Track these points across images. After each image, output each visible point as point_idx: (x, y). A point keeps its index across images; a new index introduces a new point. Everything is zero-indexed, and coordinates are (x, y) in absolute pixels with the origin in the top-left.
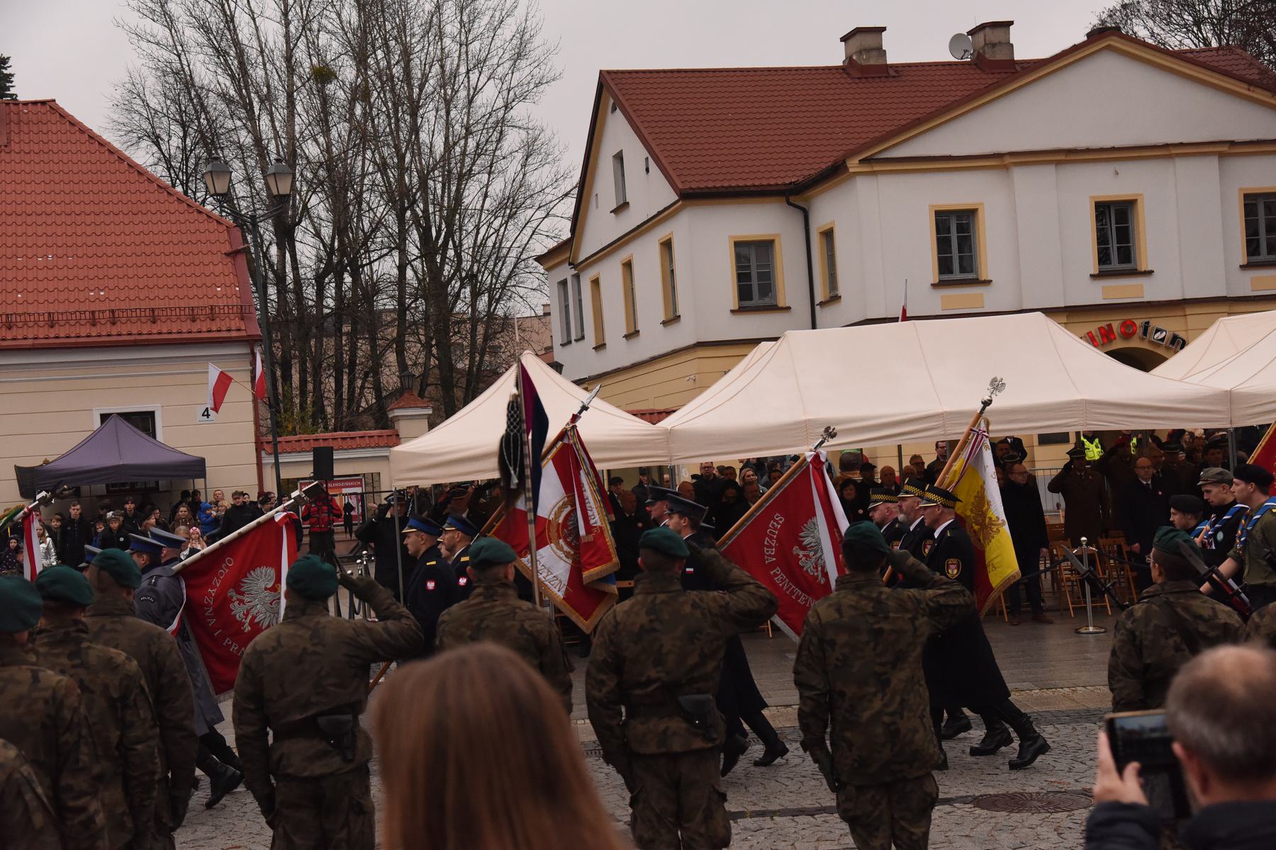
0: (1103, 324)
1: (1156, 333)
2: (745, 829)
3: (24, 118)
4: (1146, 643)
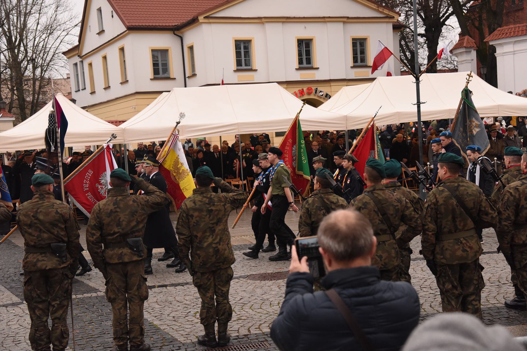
0: (300, 89)
2: (155, 292)
4: (312, 213)
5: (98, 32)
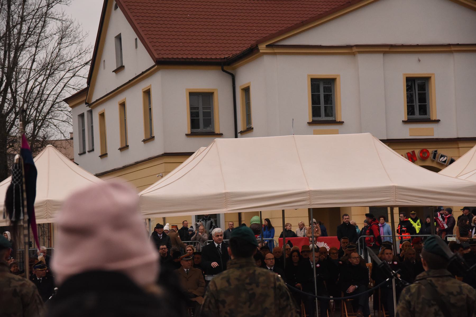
0: (410, 151)
1: (441, 158)
4: (417, 310)
5: (115, 68)
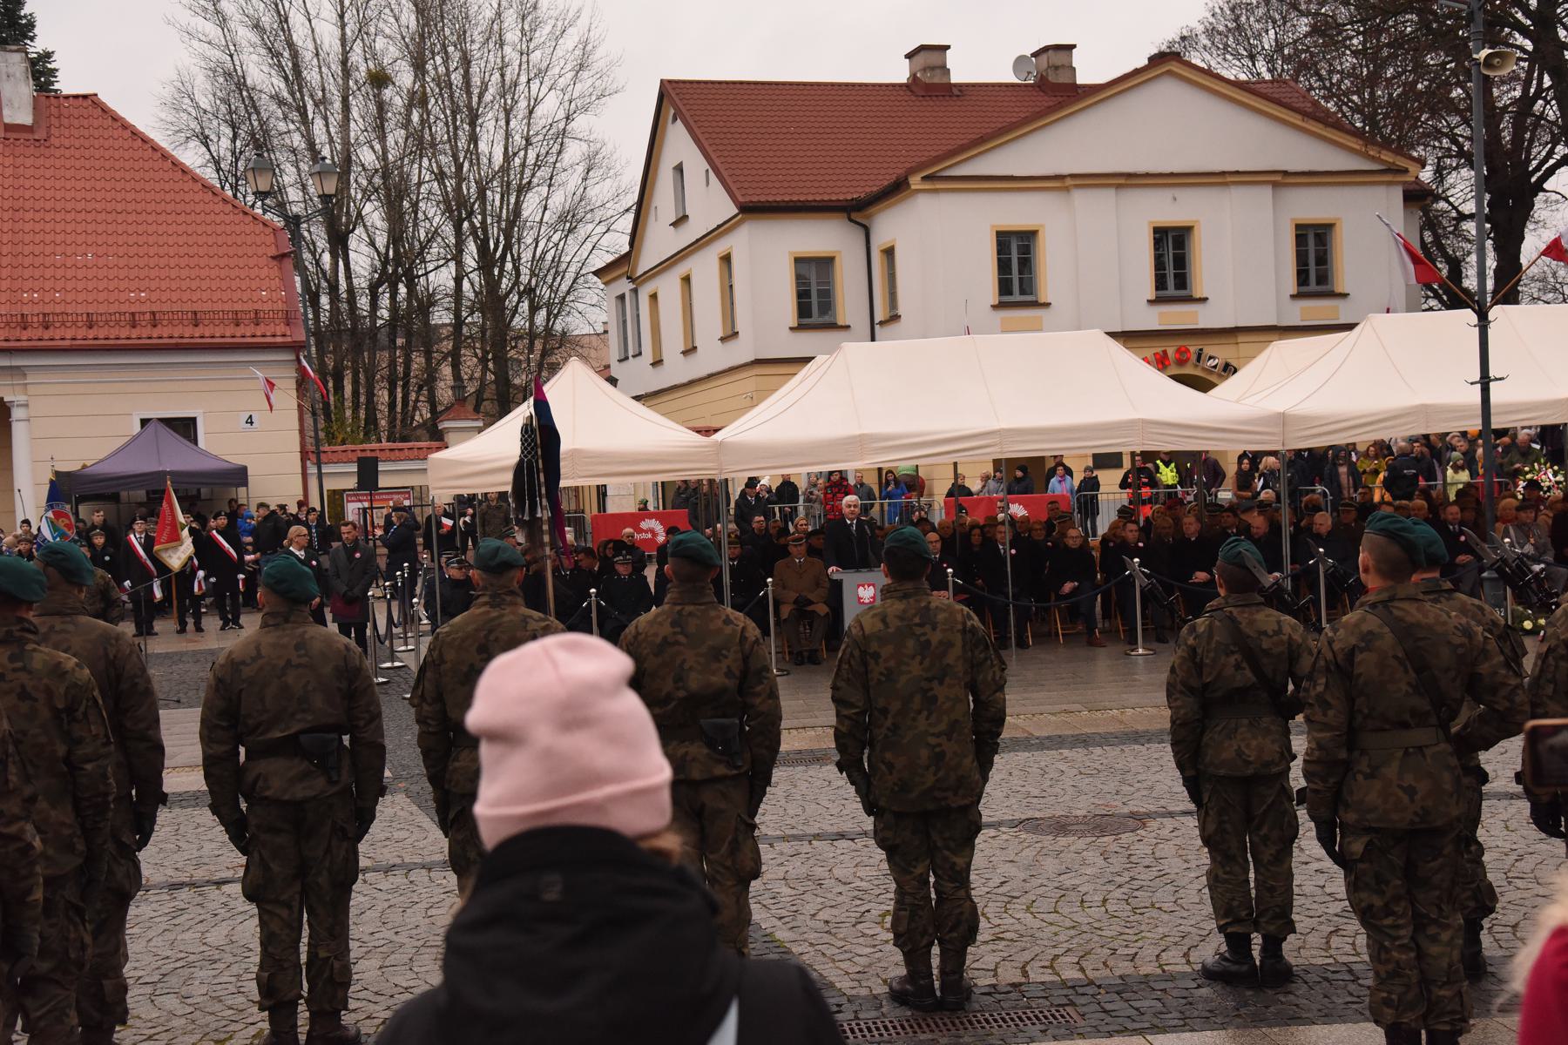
0: (1160, 350)
2: (782, 854)
3: (65, 112)
